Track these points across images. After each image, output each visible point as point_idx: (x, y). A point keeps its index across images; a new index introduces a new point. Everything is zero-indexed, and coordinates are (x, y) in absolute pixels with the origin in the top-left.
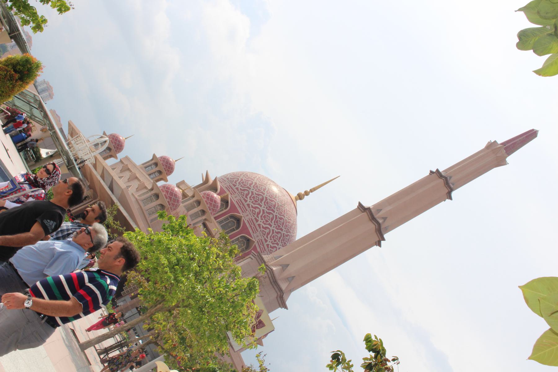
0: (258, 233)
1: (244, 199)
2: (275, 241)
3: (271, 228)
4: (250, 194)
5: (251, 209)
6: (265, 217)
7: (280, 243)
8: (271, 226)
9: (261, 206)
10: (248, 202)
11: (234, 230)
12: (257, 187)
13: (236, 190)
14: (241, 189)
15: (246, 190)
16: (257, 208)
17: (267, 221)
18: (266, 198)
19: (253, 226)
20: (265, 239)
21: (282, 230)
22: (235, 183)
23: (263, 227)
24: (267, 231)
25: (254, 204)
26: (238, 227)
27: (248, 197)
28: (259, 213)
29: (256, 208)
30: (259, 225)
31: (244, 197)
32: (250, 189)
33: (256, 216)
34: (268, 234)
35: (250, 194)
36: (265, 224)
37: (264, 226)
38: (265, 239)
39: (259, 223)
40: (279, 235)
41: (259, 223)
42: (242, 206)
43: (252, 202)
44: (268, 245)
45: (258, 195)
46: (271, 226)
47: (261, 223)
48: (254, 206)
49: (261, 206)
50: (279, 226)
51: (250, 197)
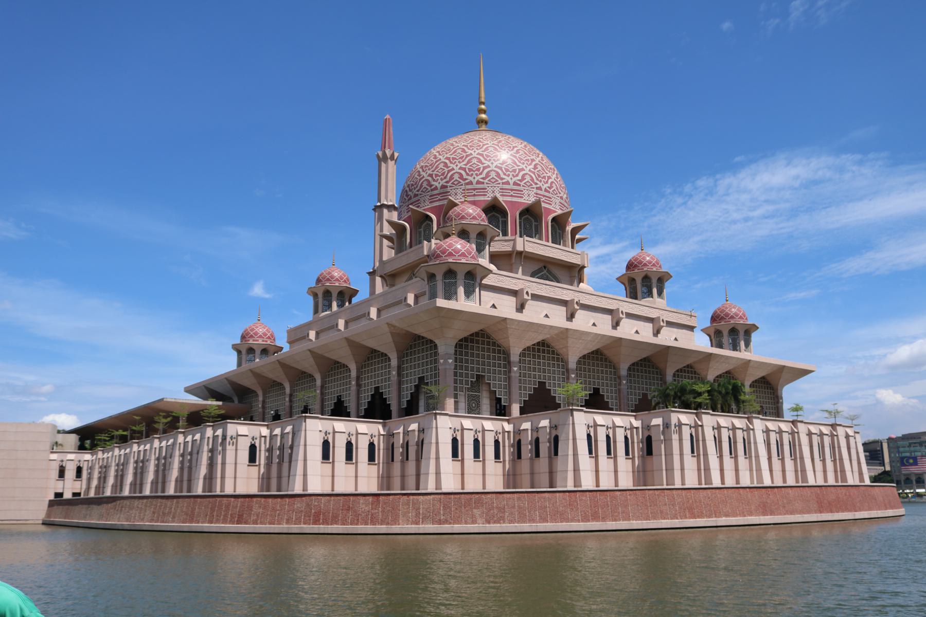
0: (526, 192)
1: (467, 184)
2: (544, 177)
3: (527, 171)
4: (463, 173)
5: (486, 181)
6: (507, 170)
7: (549, 174)
8: (523, 170)
9: (488, 167)
10: (474, 182)
11: (505, 224)
12: (454, 159)
13: (445, 190)
14: (447, 182)
15: (452, 175)
16: (489, 172)
17: (514, 171)
18: (478, 154)
19: (512, 193)
20: (537, 188)
21: (533, 160)
22: (431, 186)
23: (520, 181)
24: (528, 178)
25: (481, 174)
26: (504, 213)
27: (465, 176)
28: (498, 175)
29: (488, 175)
30: (515, 184)
31: (463, 182)
32: (453, 169)
33: (500, 181)
34: (532, 180)
35: (463, 173)
36: (517, 175)
37: (519, 178)
38: (537, 188)
39: (511, 183)
40: (540, 168)
41: (511, 183)
42: (475, 192)
43: (477, 175)
44: (546, 190)
45: (469, 162)
46: (523, 170)
47: (515, 179)
48: (483, 175)
49: (488, 167)
50: (528, 160)
51: (468, 174)
